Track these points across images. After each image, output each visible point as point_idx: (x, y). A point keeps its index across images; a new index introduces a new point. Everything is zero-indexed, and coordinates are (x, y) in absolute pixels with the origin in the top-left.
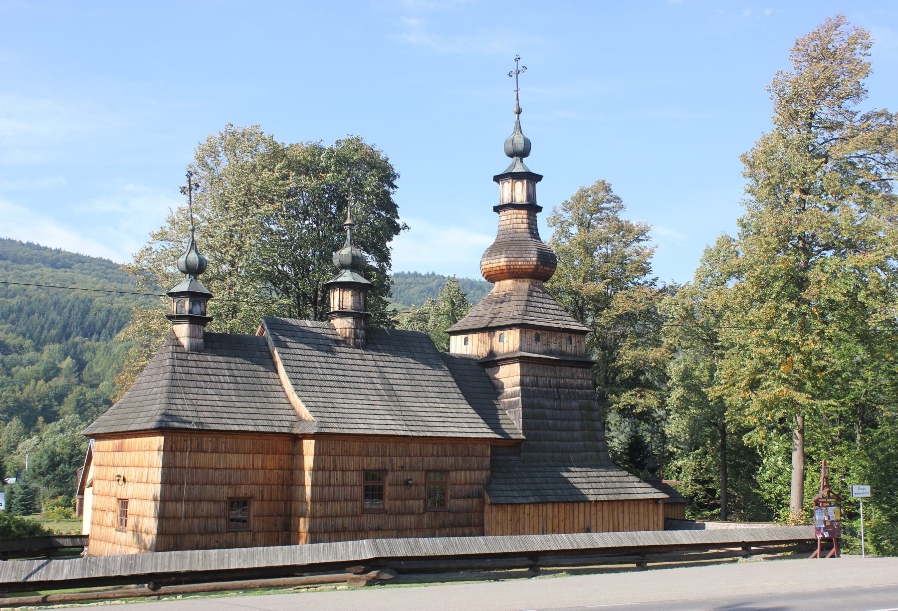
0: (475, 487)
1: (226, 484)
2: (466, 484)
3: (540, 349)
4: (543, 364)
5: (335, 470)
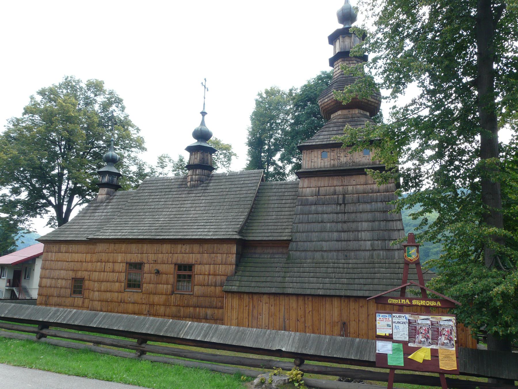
0: (218, 278)
1: (71, 270)
2: (209, 275)
3: (326, 164)
4: (328, 176)
5: (108, 262)
